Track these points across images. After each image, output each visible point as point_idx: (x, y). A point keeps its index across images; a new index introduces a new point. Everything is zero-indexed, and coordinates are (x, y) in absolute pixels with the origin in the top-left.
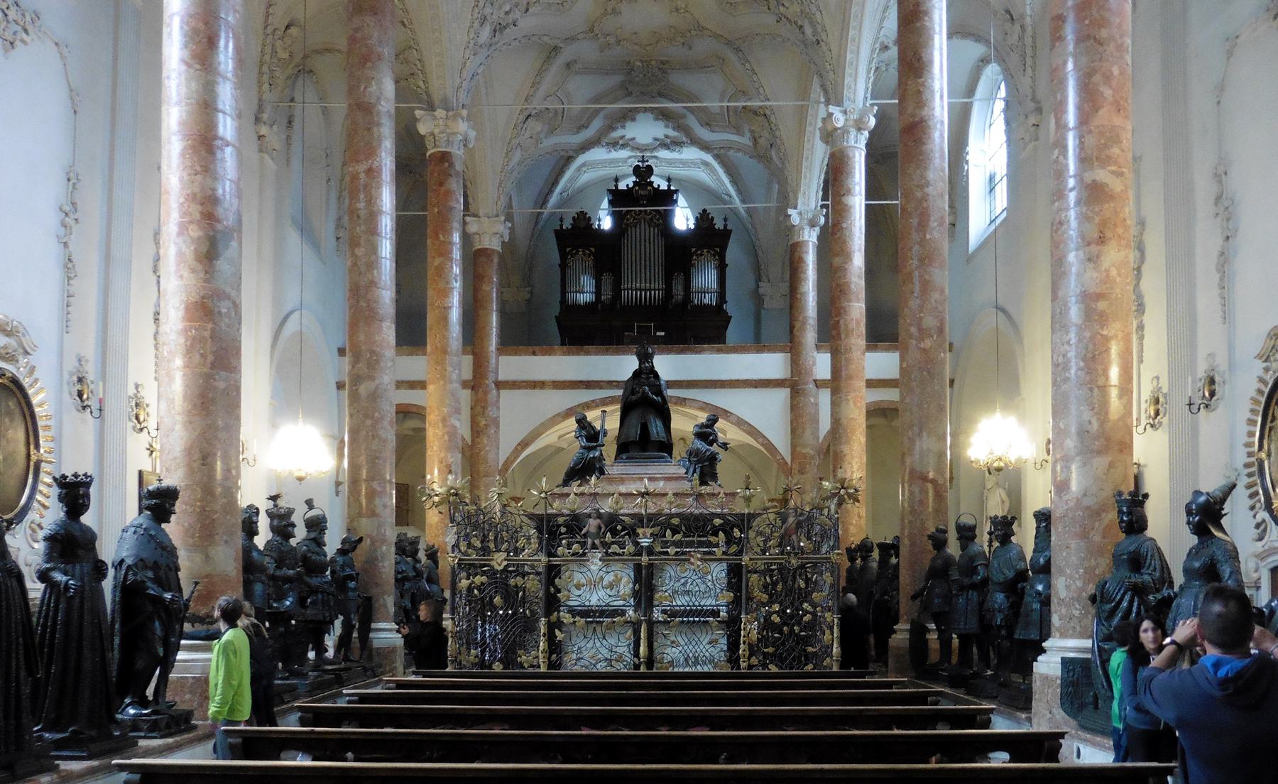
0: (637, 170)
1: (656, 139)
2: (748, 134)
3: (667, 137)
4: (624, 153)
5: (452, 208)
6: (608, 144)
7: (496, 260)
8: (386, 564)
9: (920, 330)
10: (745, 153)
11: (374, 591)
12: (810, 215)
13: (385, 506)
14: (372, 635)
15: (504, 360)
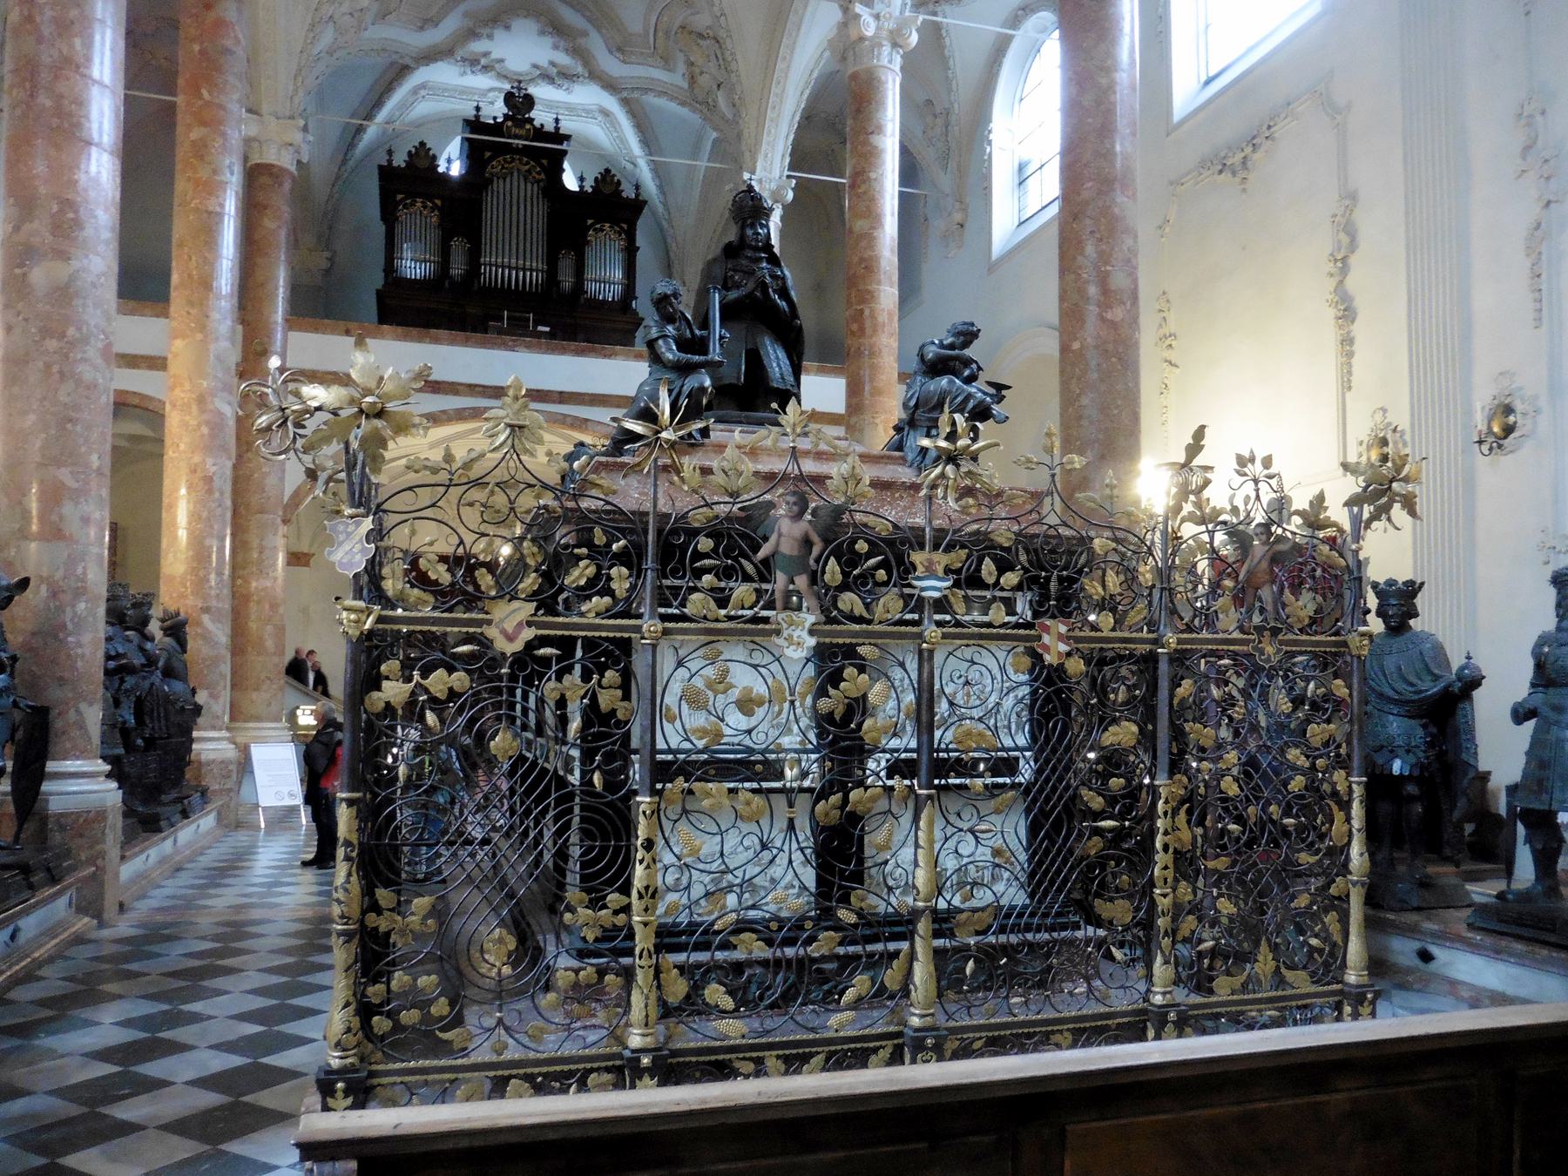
0: (509, 98)
1: (535, 66)
2: (681, 67)
3: (553, 64)
4: (482, 81)
5: (227, 51)
6: (464, 60)
7: (287, 186)
8: (86, 638)
9: (1105, 291)
10: (672, 98)
11: (53, 694)
12: (773, 186)
13: (86, 520)
14: (46, 787)
15: (296, 337)
